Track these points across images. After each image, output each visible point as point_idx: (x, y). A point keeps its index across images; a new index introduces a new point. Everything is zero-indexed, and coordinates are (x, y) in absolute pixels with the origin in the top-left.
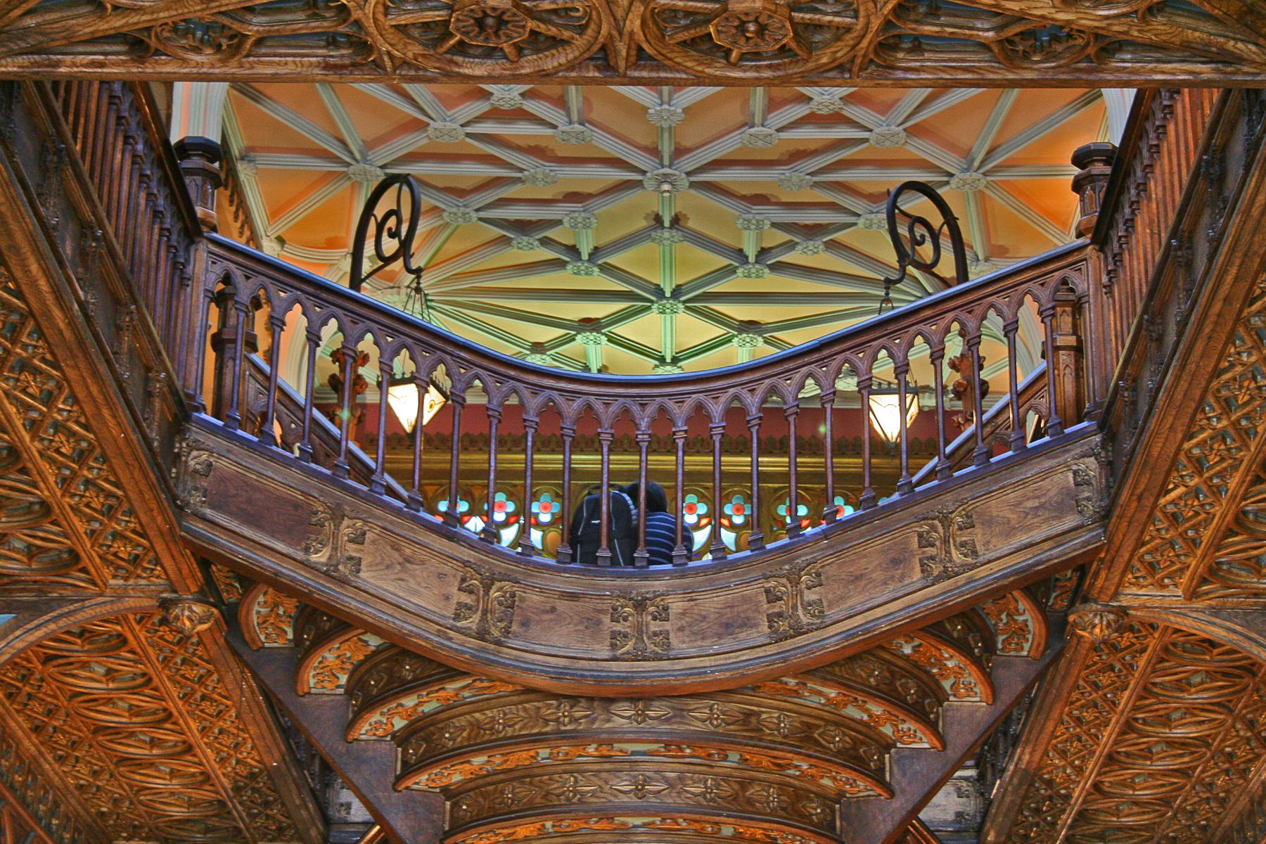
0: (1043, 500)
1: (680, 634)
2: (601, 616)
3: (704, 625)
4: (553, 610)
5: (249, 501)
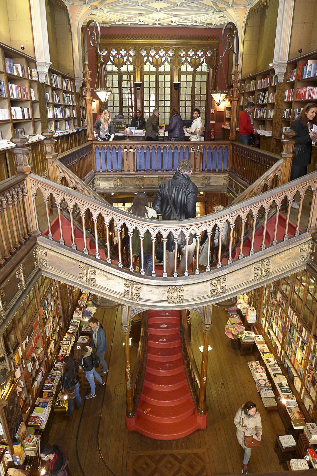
0: (290, 257)
1: (186, 296)
2: (164, 292)
3: (193, 293)
4: (151, 291)
5: (60, 263)
